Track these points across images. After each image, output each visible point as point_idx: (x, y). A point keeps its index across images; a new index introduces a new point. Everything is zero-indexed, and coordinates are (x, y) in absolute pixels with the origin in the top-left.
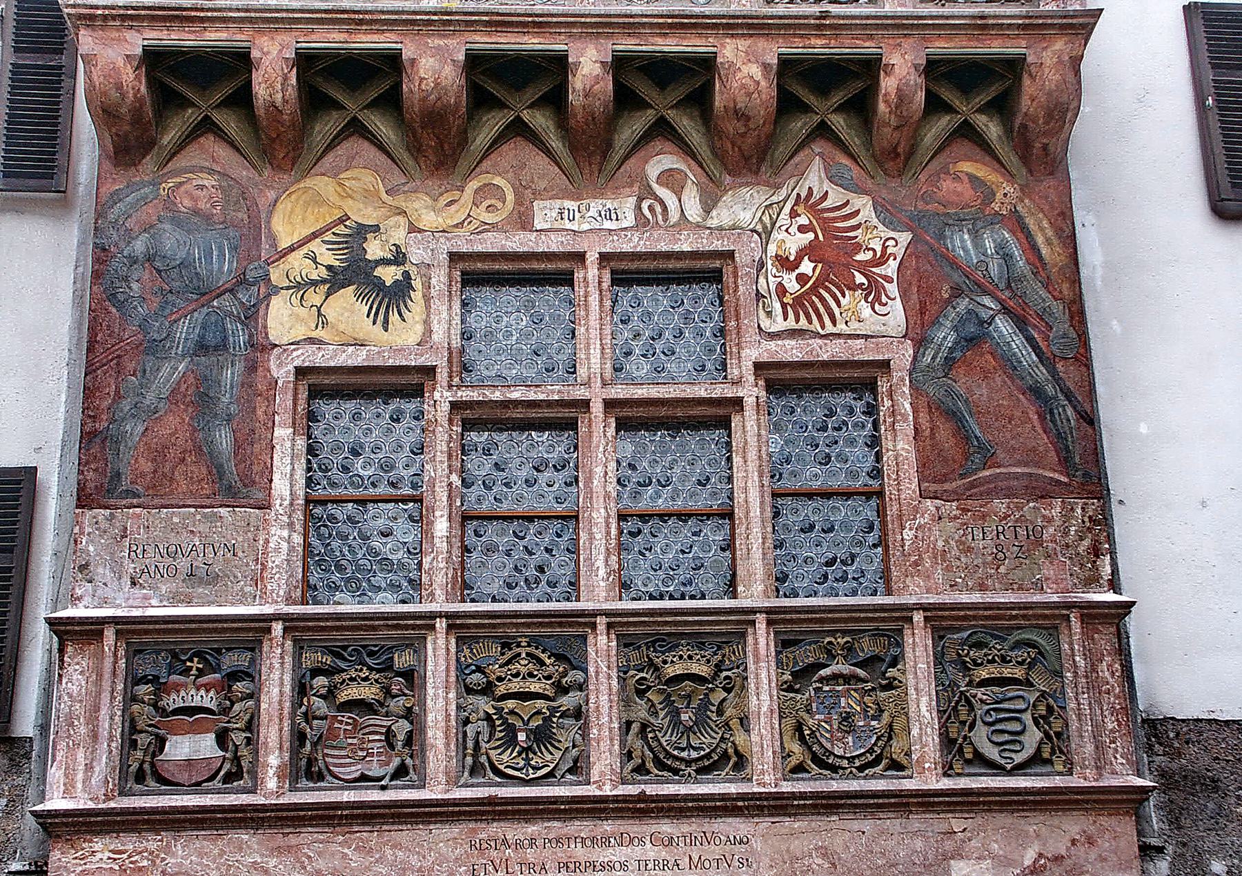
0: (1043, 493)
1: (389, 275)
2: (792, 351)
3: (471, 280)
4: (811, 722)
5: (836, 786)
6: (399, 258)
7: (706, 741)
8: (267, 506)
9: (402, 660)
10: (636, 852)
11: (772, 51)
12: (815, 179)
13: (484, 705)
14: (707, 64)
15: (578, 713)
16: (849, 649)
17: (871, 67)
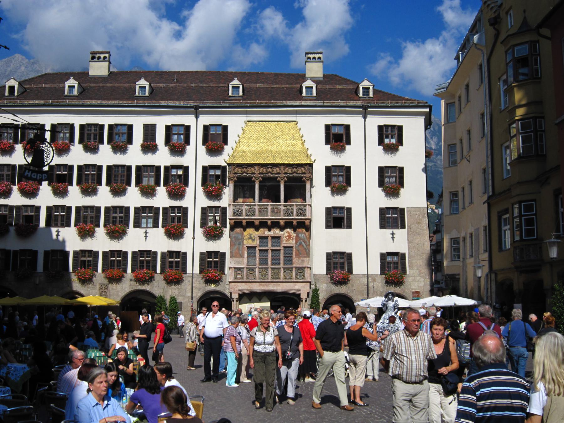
0: (305, 257)
1: (253, 238)
2: (286, 245)
3: (260, 238)
5: (287, 280)
6: (254, 237)
7: (277, 277)
8: (244, 258)
11: (284, 221)
13: (261, 274)
17: (292, 222)
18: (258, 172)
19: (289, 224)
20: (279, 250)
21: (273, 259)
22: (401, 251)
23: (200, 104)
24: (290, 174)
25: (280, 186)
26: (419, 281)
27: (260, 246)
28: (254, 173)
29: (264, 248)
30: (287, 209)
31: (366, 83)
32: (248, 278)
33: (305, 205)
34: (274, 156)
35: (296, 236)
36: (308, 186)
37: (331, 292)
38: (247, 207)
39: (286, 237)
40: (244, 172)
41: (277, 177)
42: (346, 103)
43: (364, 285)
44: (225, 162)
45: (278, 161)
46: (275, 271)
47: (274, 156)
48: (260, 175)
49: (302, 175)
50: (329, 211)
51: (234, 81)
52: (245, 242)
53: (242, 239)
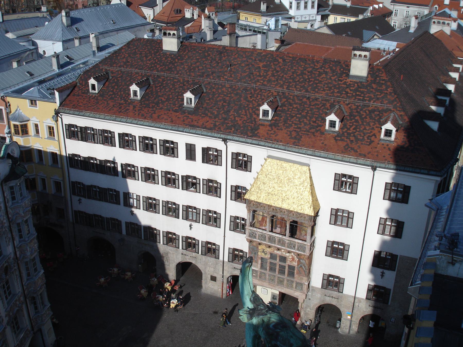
0: (303, 276)
2: (290, 264)
32: (260, 277)
34: (283, 200)
35: (298, 260)
37: (324, 301)
47: (283, 200)
51: (264, 105)
52: (259, 253)
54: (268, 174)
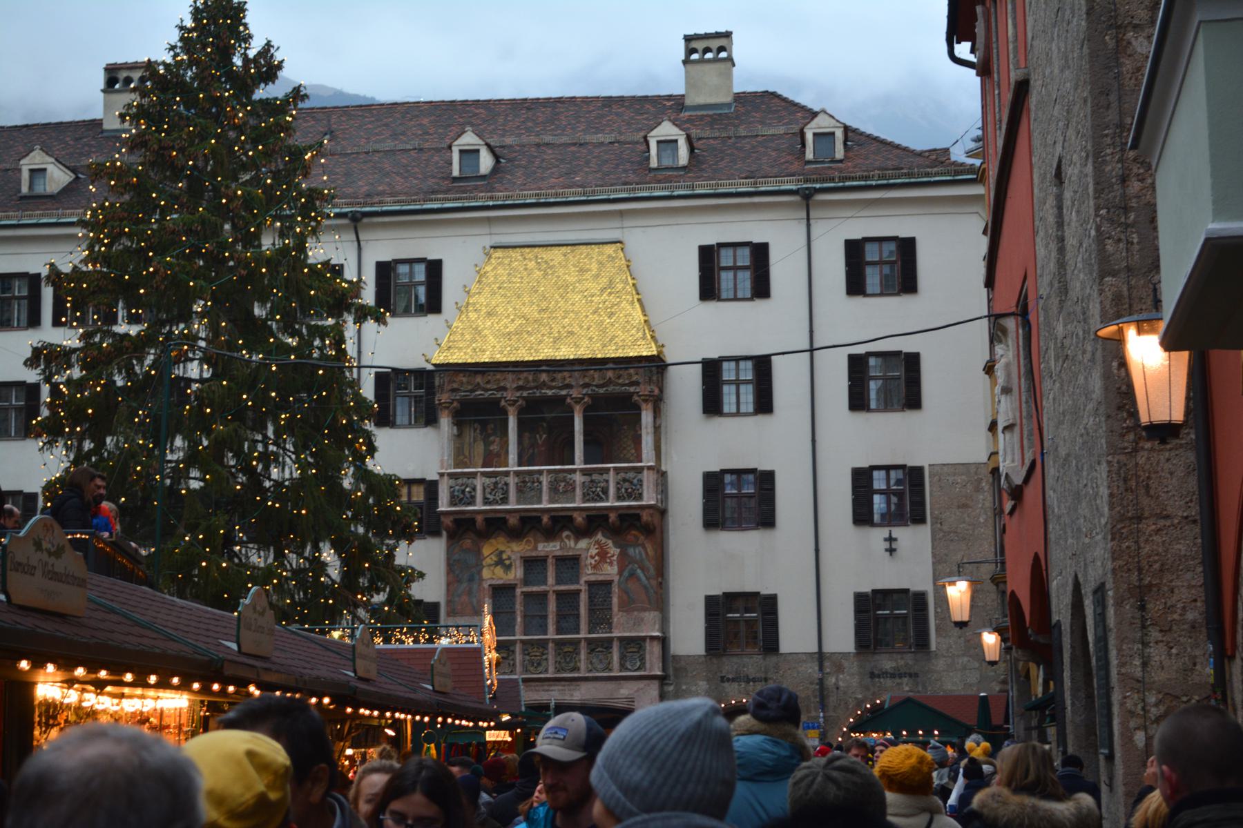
0: (644, 610)
1: (507, 562)
2: (593, 578)
4: (594, 661)
6: (509, 558)
7: (572, 665)
9: (511, 648)
10: (556, 688)
11: (584, 514)
12: (599, 536)
13: (527, 657)
14: (571, 516)
15: (546, 659)
16: (602, 646)
18: (515, 386)
19: (595, 522)
20: (578, 592)
21: (560, 617)
22: (916, 587)
23: (366, 204)
24: (597, 386)
25: (572, 419)
26: (964, 668)
27: (526, 582)
28: (504, 389)
29: (535, 589)
30: (592, 481)
31: (820, 124)
33: (639, 470)
35: (620, 554)
36: (647, 417)
38: (487, 481)
39: (592, 557)
40: (478, 387)
41: (564, 398)
42: (755, 183)
43: (811, 683)
44: (427, 361)
45: (565, 352)
46: (567, 650)
48: (518, 394)
49: (632, 389)
50: (713, 482)
51: (464, 136)
52: (486, 573)
53: (477, 565)
54: (499, 288)
